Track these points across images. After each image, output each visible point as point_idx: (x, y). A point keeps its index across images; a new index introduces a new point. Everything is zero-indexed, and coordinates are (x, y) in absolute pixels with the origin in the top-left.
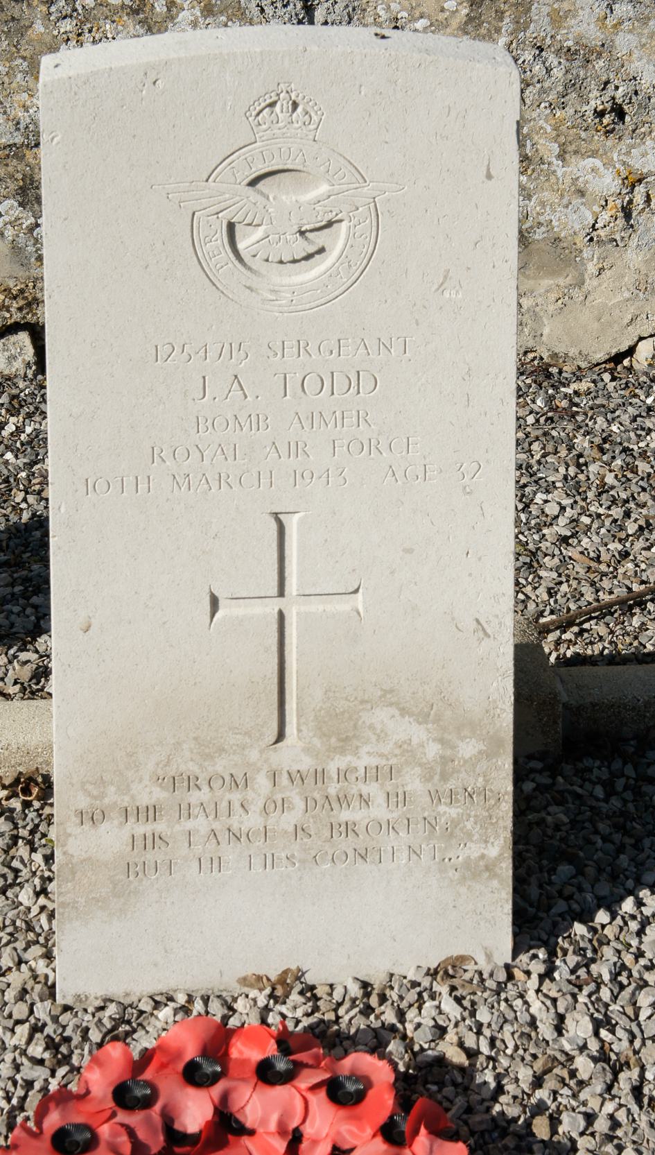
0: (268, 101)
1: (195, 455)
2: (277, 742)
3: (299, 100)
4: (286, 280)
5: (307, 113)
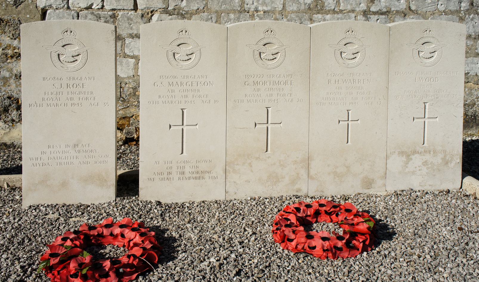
1: (167, 97)
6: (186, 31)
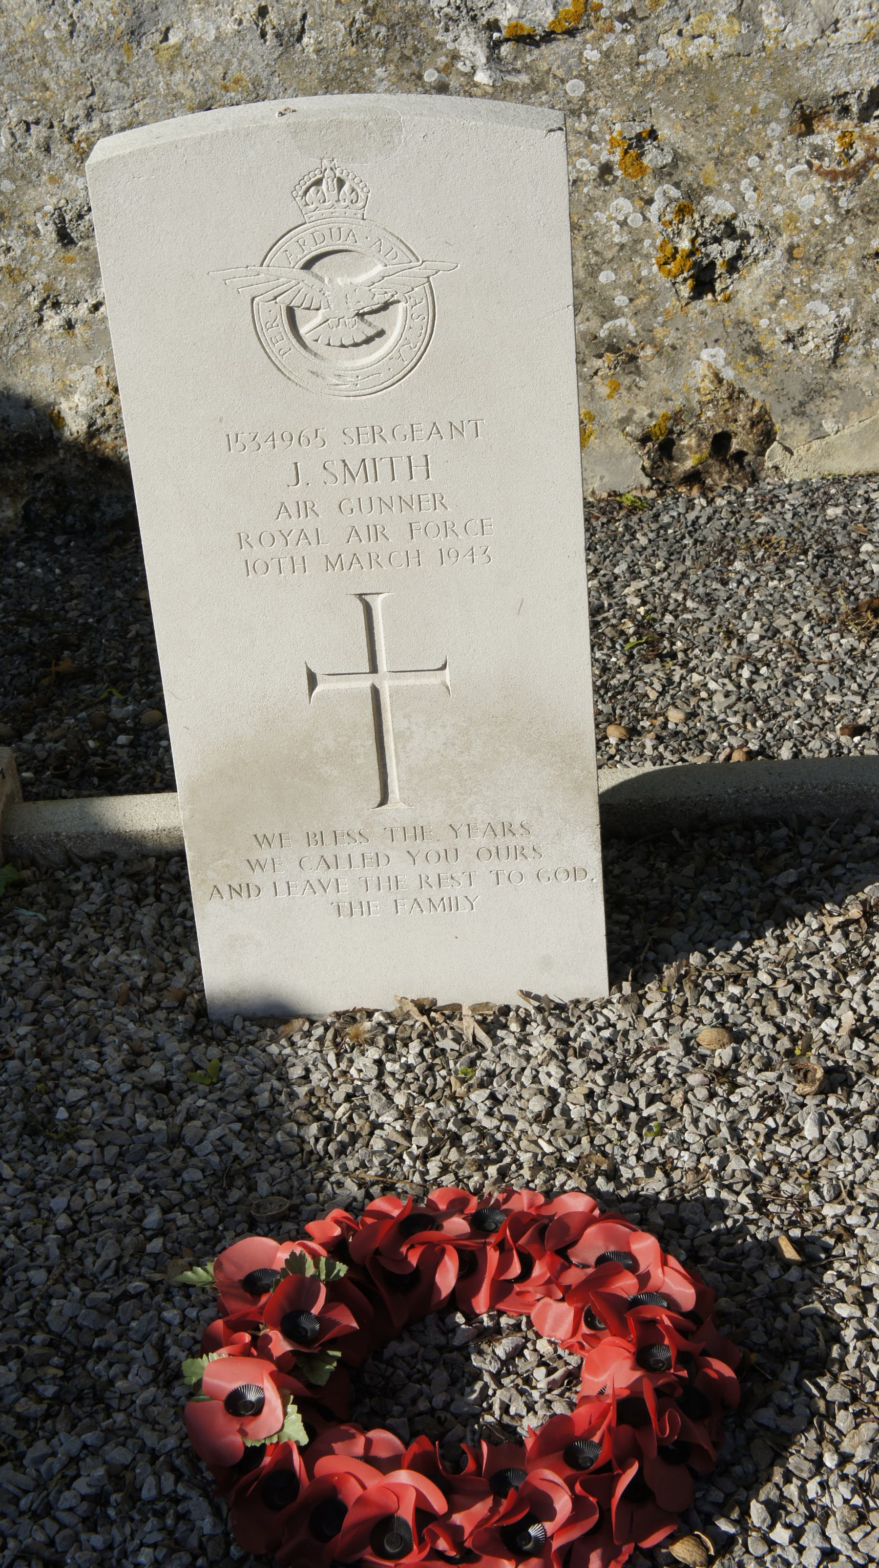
1: (280, 539)
3: (343, 176)
4: (348, 364)
5: (353, 190)
6: (341, 183)
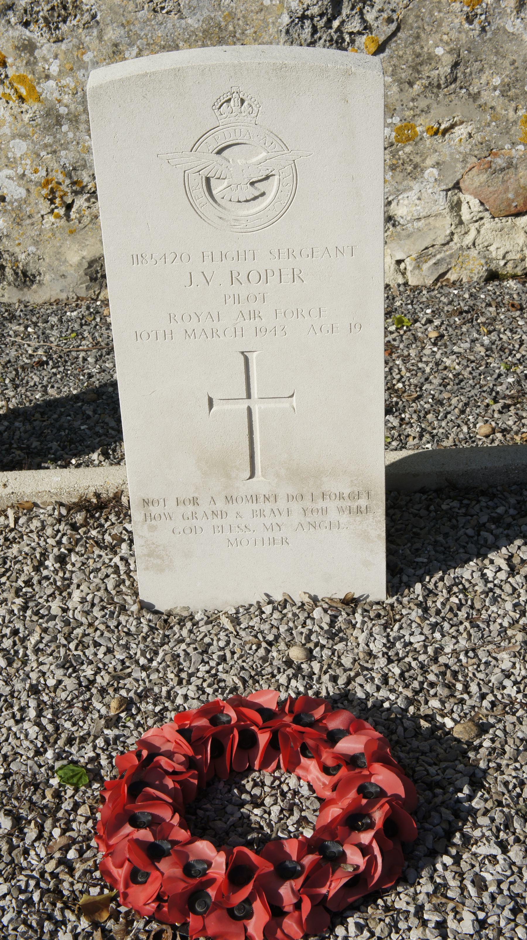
0: (226, 99)
1: (195, 319)
2: (250, 478)
3: (244, 98)
6: (243, 101)
